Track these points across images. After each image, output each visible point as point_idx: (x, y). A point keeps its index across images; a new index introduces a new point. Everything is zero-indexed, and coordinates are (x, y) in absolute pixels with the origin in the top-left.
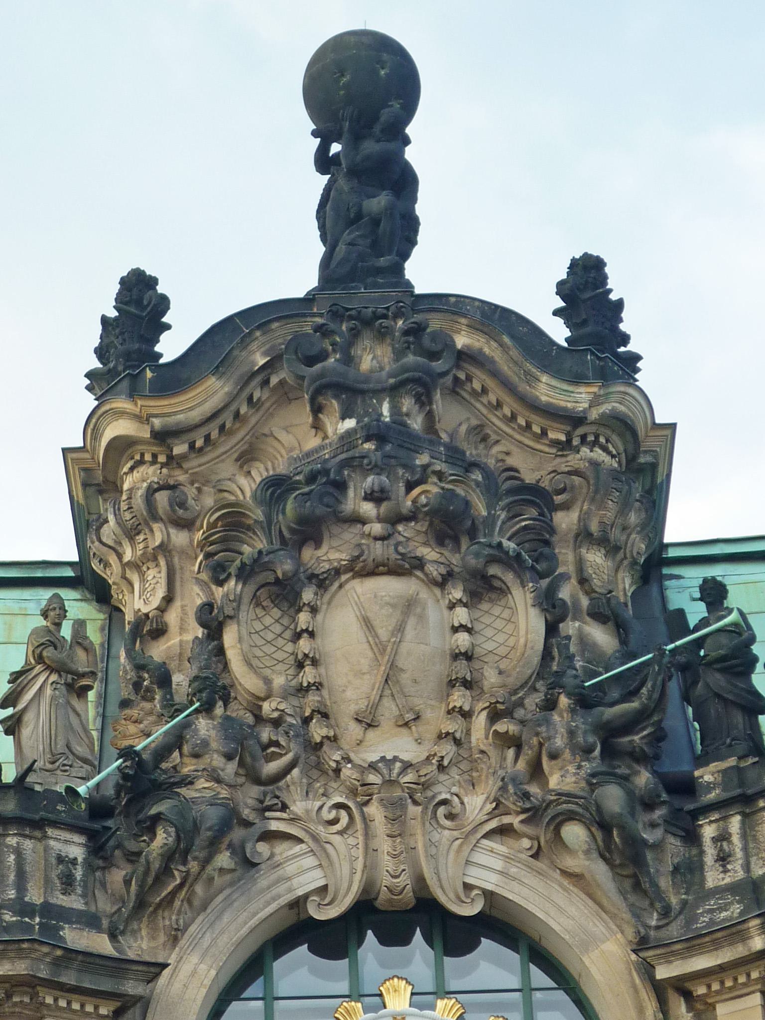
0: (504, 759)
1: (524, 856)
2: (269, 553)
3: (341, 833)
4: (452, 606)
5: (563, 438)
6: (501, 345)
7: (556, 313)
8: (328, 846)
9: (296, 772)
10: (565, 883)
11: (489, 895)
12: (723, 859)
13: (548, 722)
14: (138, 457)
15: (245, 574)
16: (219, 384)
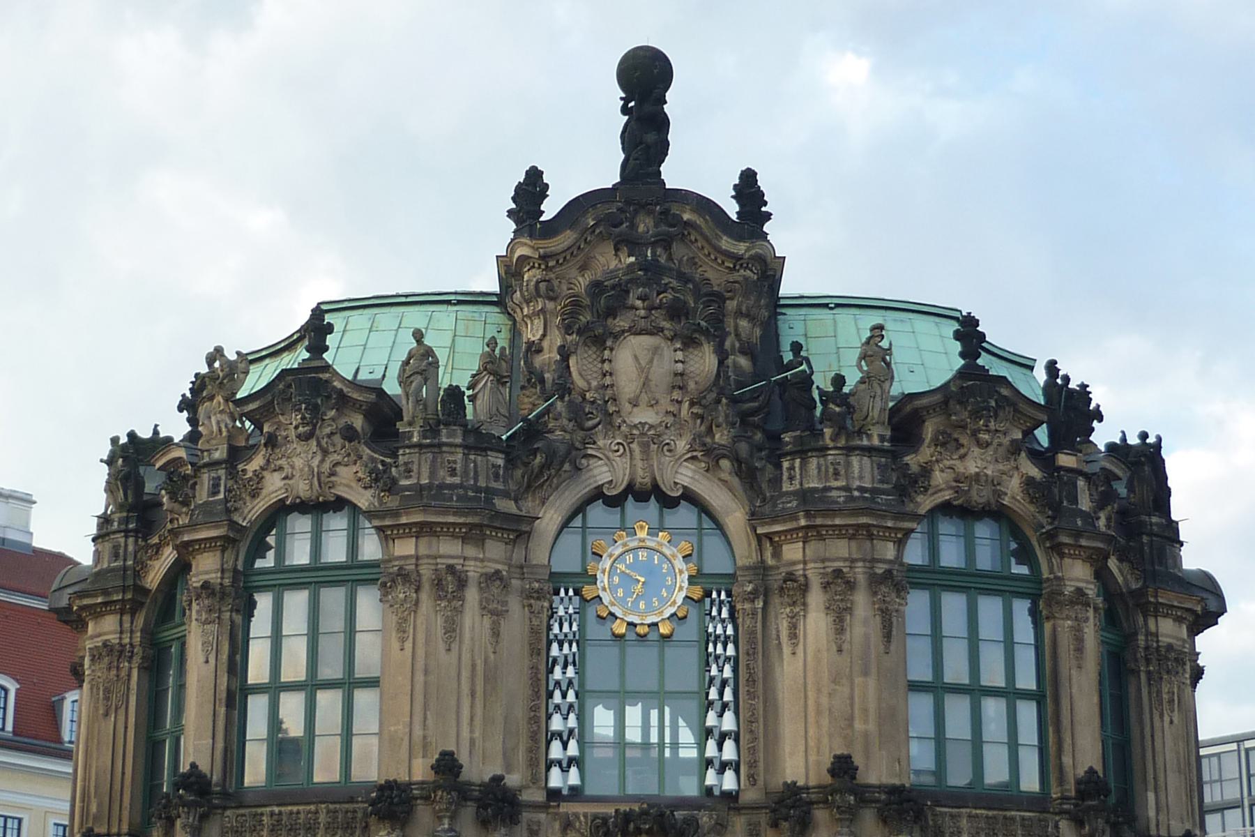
0: (695, 424)
1: (702, 471)
2: (592, 323)
3: (620, 456)
4: (675, 351)
5: (732, 266)
6: (705, 219)
7: (732, 197)
8: (614, 463)
9: (600, 426)
10: (720, 483)
11: (685, 487)
12: (791, 478)
13: (716, 410)
14: (531, 264)
15: (579, 333)
16: (571, 233)
